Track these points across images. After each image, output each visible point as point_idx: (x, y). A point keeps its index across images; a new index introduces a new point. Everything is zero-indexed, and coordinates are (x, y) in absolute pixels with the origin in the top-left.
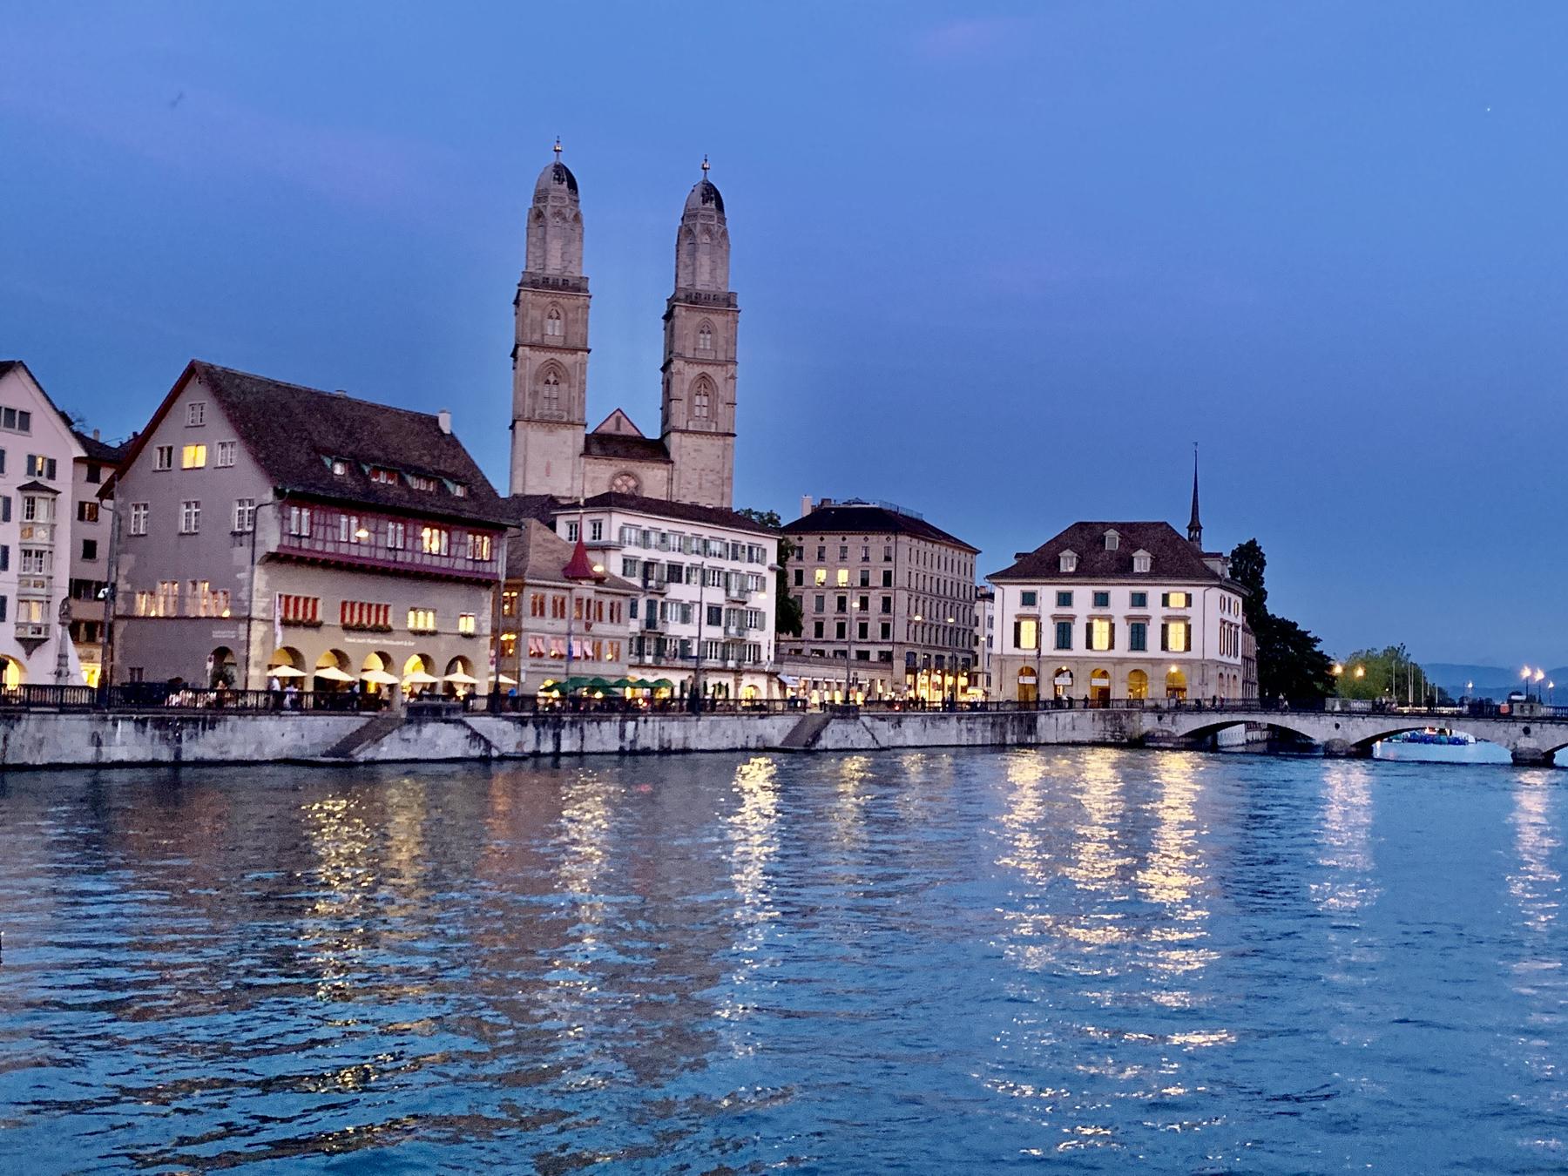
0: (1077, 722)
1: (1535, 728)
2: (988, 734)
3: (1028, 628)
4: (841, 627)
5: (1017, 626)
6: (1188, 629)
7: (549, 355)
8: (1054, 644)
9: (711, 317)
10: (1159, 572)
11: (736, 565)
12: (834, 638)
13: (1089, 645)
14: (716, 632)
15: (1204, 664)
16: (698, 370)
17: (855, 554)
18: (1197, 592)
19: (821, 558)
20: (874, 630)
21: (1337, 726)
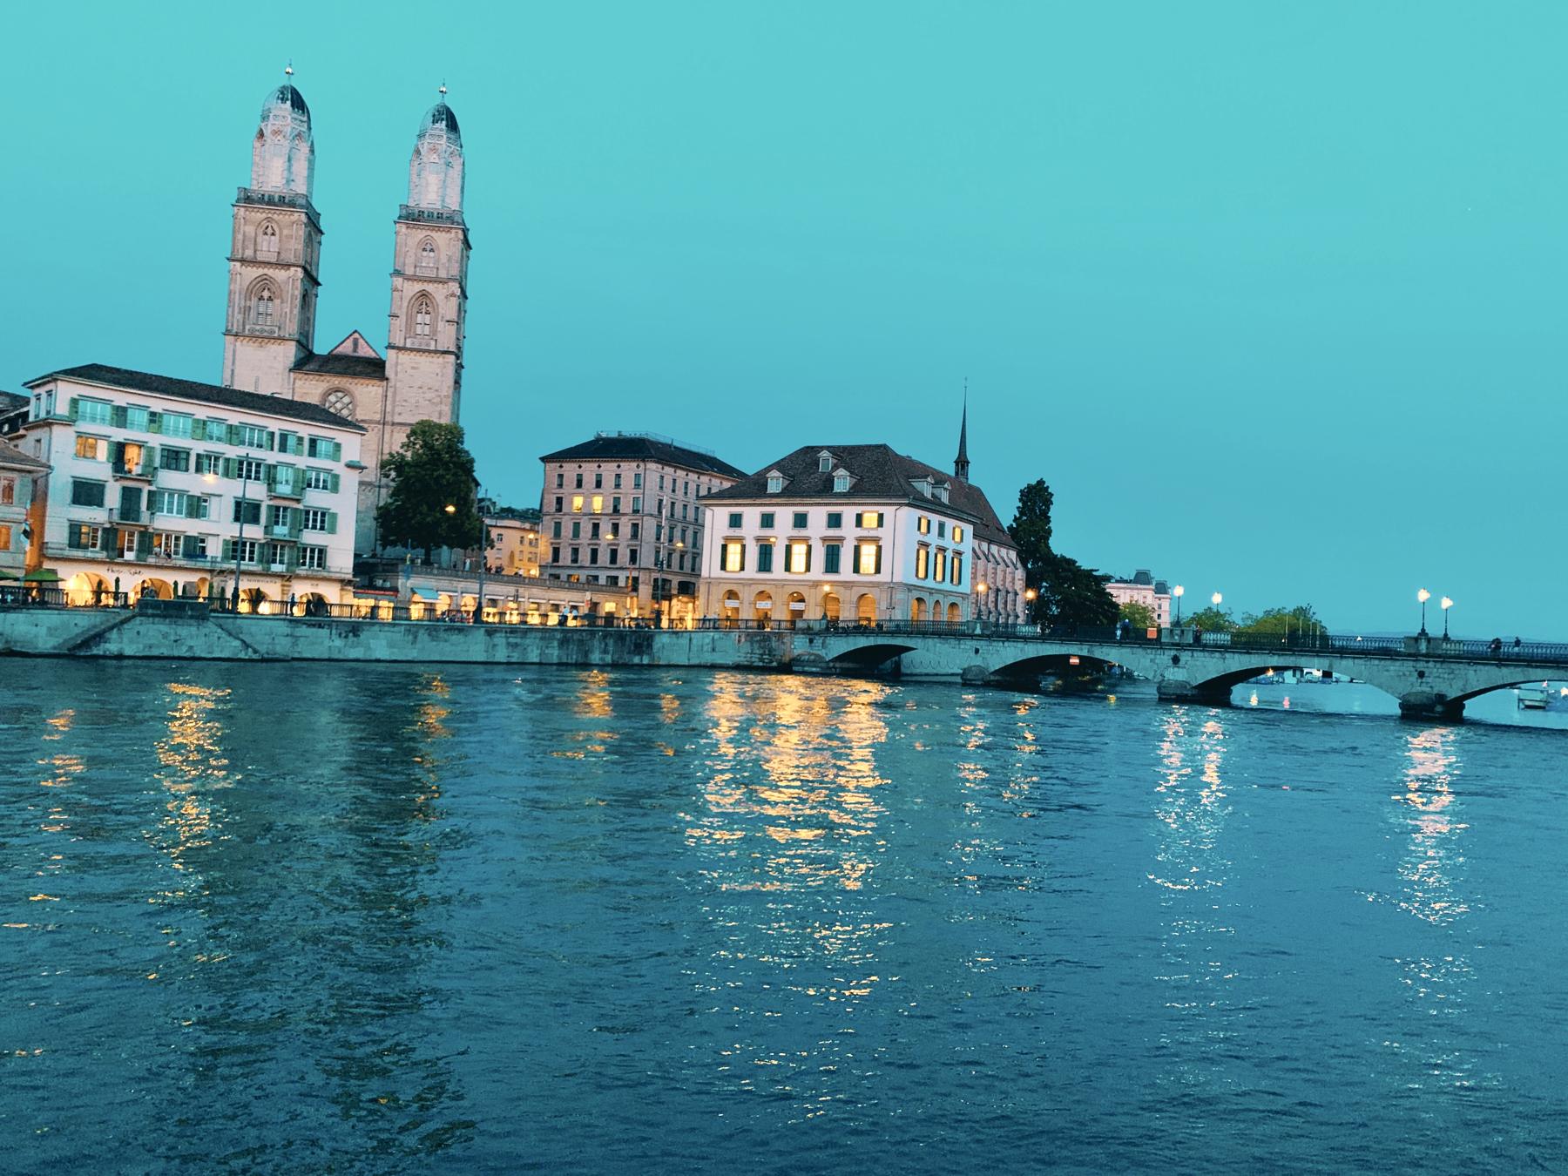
0: (718, 644)
1: (1185, 657)
2: (556, 652)
3: (734, 550)
4: (594, 553)
5: (724, 548)
6: (879, 549)
7: (261, 271)
8: (756, 567)
9: (434, 234)
10: (858, 492)
11: (287, 458)
12: (588, 564)
13: (788, 568)
14: (254, 532)
15: (892, 587)
16: (418, 287)
17: (609, 481)
18: (888, 511)
19: (579, 484)
20: (624, 556)
21: (977, 651)
